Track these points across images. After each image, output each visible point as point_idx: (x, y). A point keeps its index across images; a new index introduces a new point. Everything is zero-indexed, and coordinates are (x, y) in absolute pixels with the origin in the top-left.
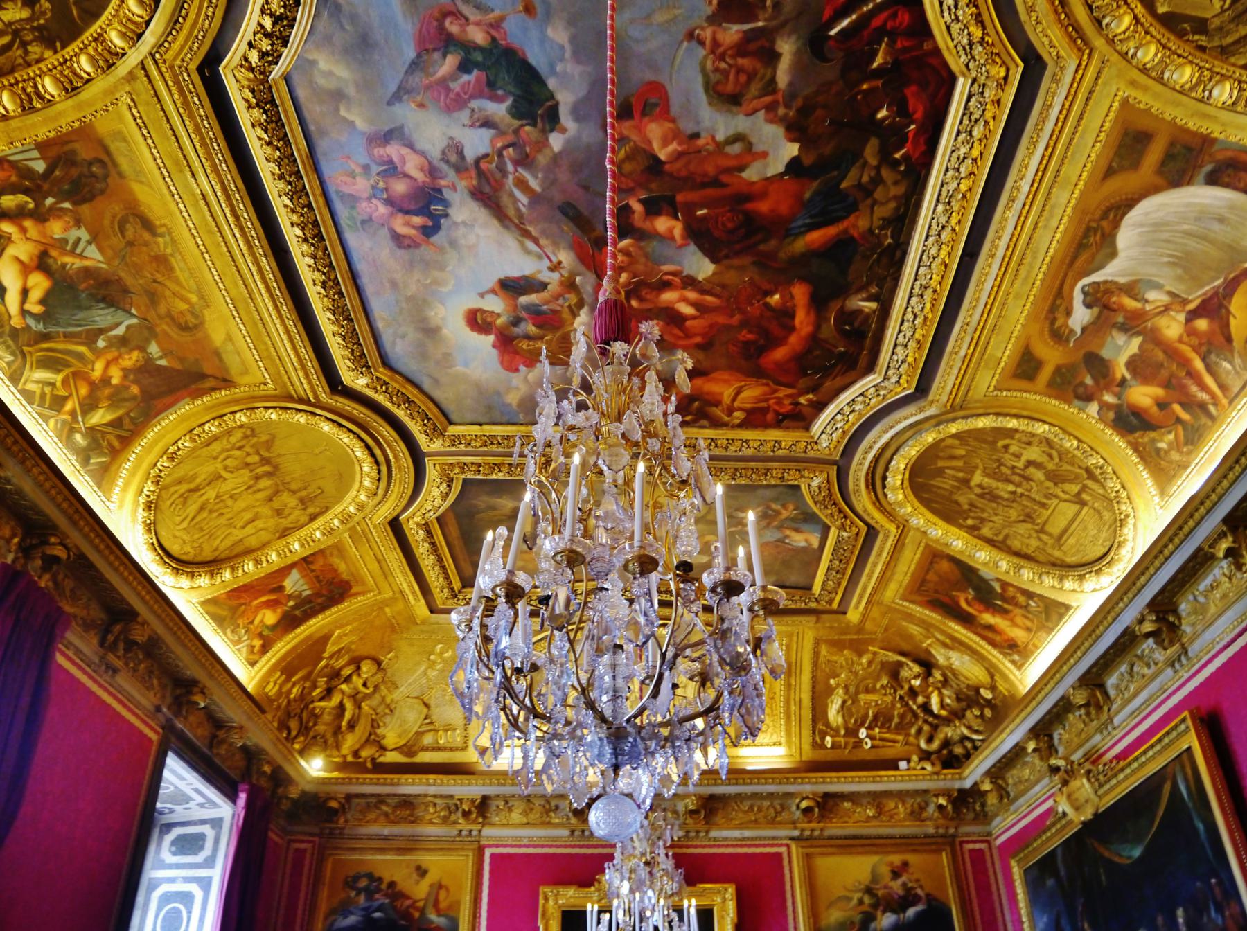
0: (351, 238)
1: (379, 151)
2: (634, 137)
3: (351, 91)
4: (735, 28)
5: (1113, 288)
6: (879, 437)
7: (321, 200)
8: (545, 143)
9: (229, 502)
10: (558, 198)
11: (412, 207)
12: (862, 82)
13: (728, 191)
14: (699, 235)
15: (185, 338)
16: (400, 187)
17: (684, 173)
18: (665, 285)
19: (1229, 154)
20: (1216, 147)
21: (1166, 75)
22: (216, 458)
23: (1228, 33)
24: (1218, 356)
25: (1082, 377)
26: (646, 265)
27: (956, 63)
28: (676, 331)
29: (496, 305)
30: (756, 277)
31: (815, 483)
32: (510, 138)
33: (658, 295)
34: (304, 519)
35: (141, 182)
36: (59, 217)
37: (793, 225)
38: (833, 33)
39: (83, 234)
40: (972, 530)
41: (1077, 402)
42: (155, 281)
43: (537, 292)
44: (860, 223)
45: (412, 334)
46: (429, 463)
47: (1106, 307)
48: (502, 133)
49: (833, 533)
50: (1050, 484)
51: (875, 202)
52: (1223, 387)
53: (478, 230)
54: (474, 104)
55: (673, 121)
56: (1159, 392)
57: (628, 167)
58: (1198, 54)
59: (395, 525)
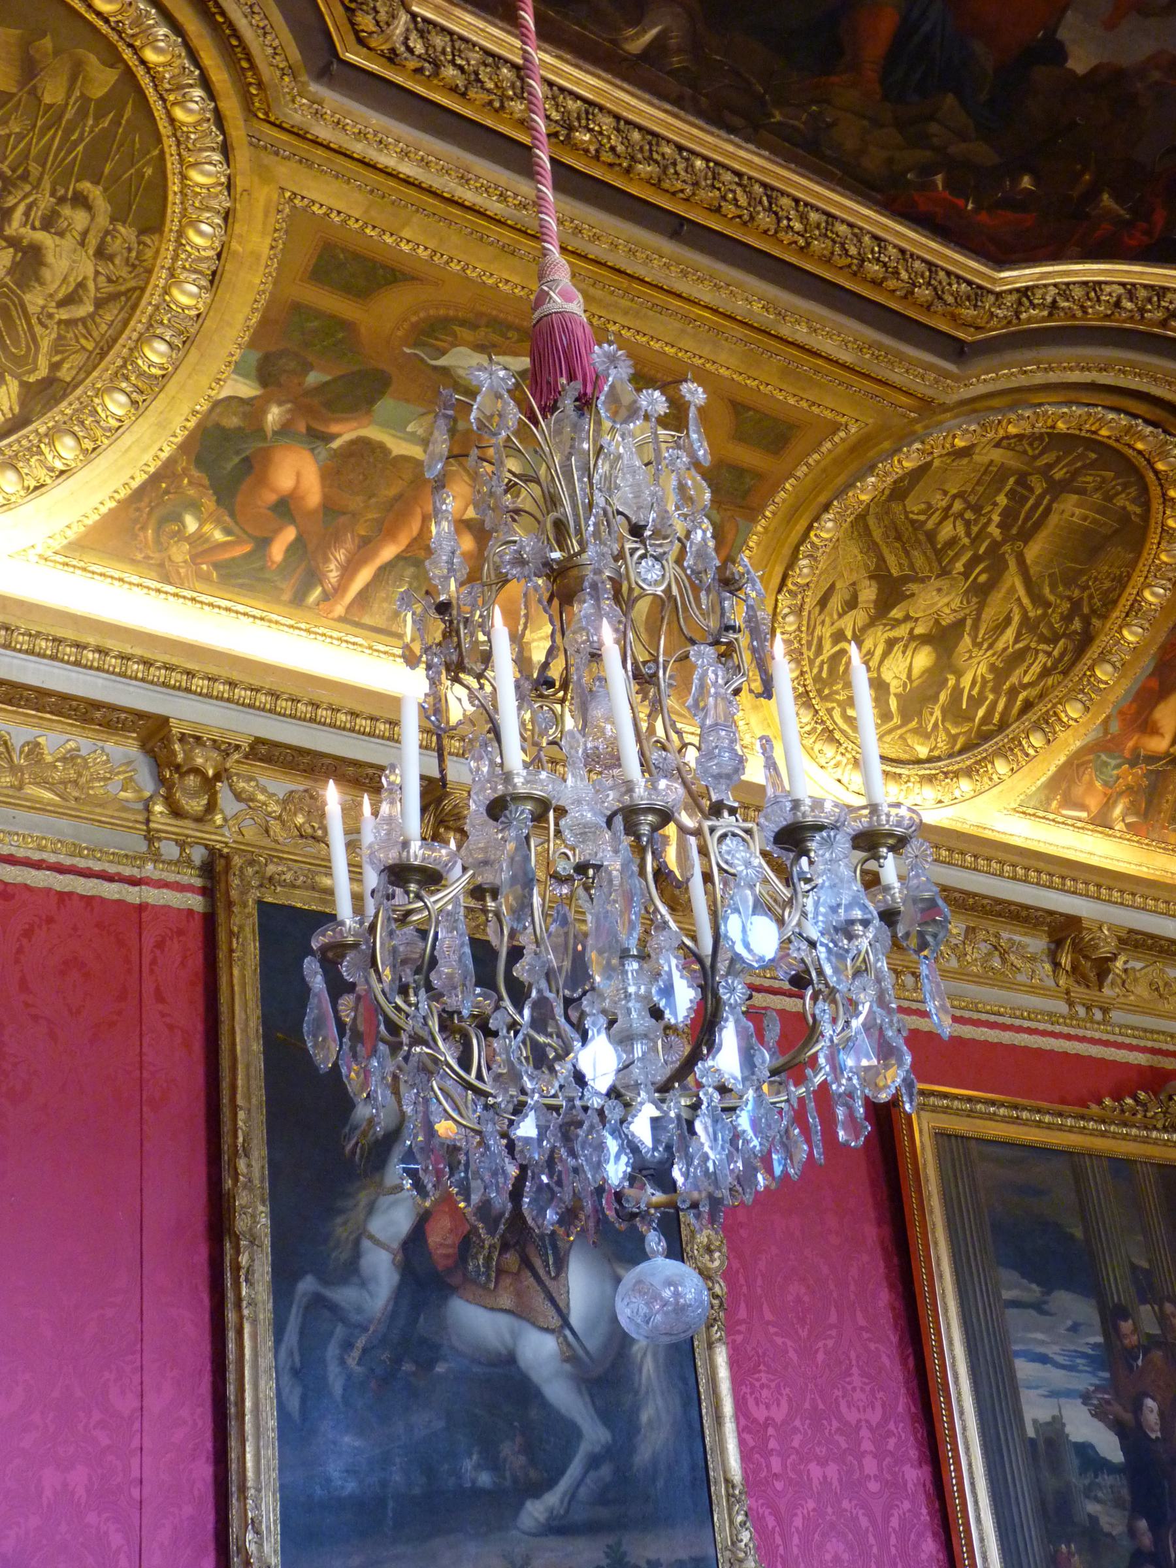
23: (879, 519)
41: (254, 357)
52: (364, 597)
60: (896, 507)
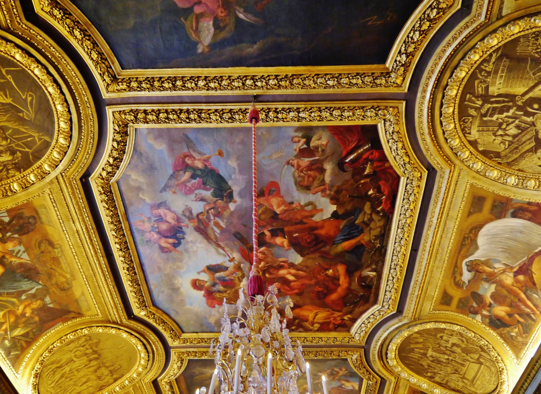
0: (141, 249)
1: (155, 212)
2: (266, 204)
3: (145, 187)
4: (307, 160)
5: (479, 263)
6: (382, 334)
7: (129, 232)
8: (228, 207)
9: (76, 373)
10: (233, 230)
11: (169, 235)
12: (361, 180)
13: (307, 226)
14: (295, 244)
15: (63, 294)
16: (164, 227)
17: (287, 219)
18: (281, 267)
19: (519, 205)
20: (513, 202)
21: (487, 174)
22: (71, 351)
23: (509, 157)
24: (531, 292)
25: (471, 304)
26: (272, 259)
27: (399, 171)
28: (287, 288)
29: (205, 277)
30: (321, 263)
31: (354, 357)
32: (212, 206)
33: (278, 271)
34: (111, 381)
35: (50, 226)
36: (12, 241)
37: (337, 239)
38: (347, 161)
39: (22, 248)
40: (431, 378)
41: (471, 315)
42: (52, 269)
43: (224, 271)
44: (365, 238)
45: (167, 291)
46: (172, 352)
47: (477, 271)
48: (209, 204)
49: (365, 382)
50: (465, 355)
51: (371, 229)
53: (198, 245)
54: (197, 192)
55: (282, 197)
56: (508, 309)
57: (263, 217)
58: (499, 165)
59: (155, 383)
60: (503, 154)
